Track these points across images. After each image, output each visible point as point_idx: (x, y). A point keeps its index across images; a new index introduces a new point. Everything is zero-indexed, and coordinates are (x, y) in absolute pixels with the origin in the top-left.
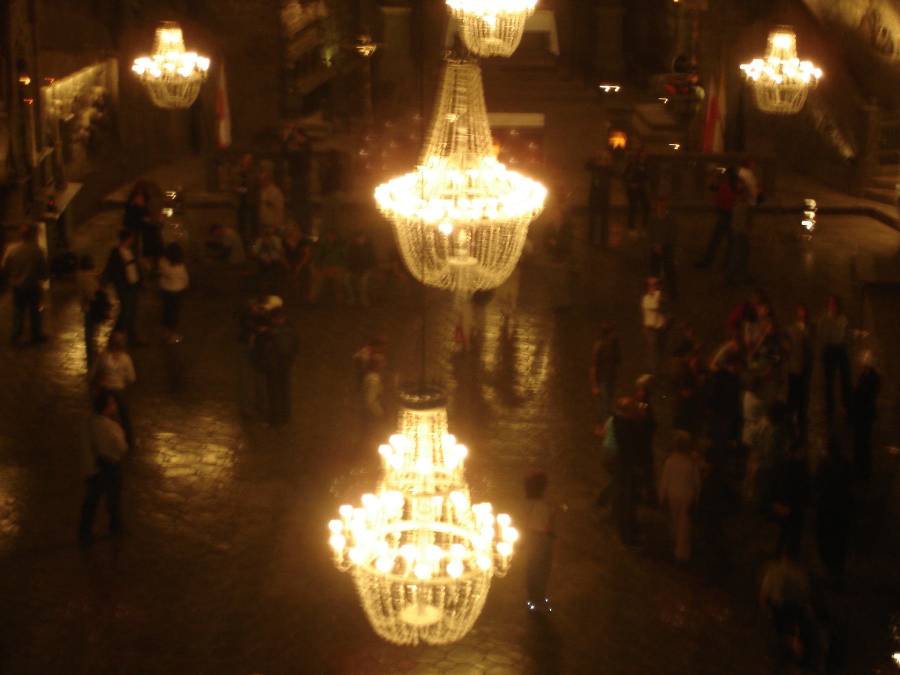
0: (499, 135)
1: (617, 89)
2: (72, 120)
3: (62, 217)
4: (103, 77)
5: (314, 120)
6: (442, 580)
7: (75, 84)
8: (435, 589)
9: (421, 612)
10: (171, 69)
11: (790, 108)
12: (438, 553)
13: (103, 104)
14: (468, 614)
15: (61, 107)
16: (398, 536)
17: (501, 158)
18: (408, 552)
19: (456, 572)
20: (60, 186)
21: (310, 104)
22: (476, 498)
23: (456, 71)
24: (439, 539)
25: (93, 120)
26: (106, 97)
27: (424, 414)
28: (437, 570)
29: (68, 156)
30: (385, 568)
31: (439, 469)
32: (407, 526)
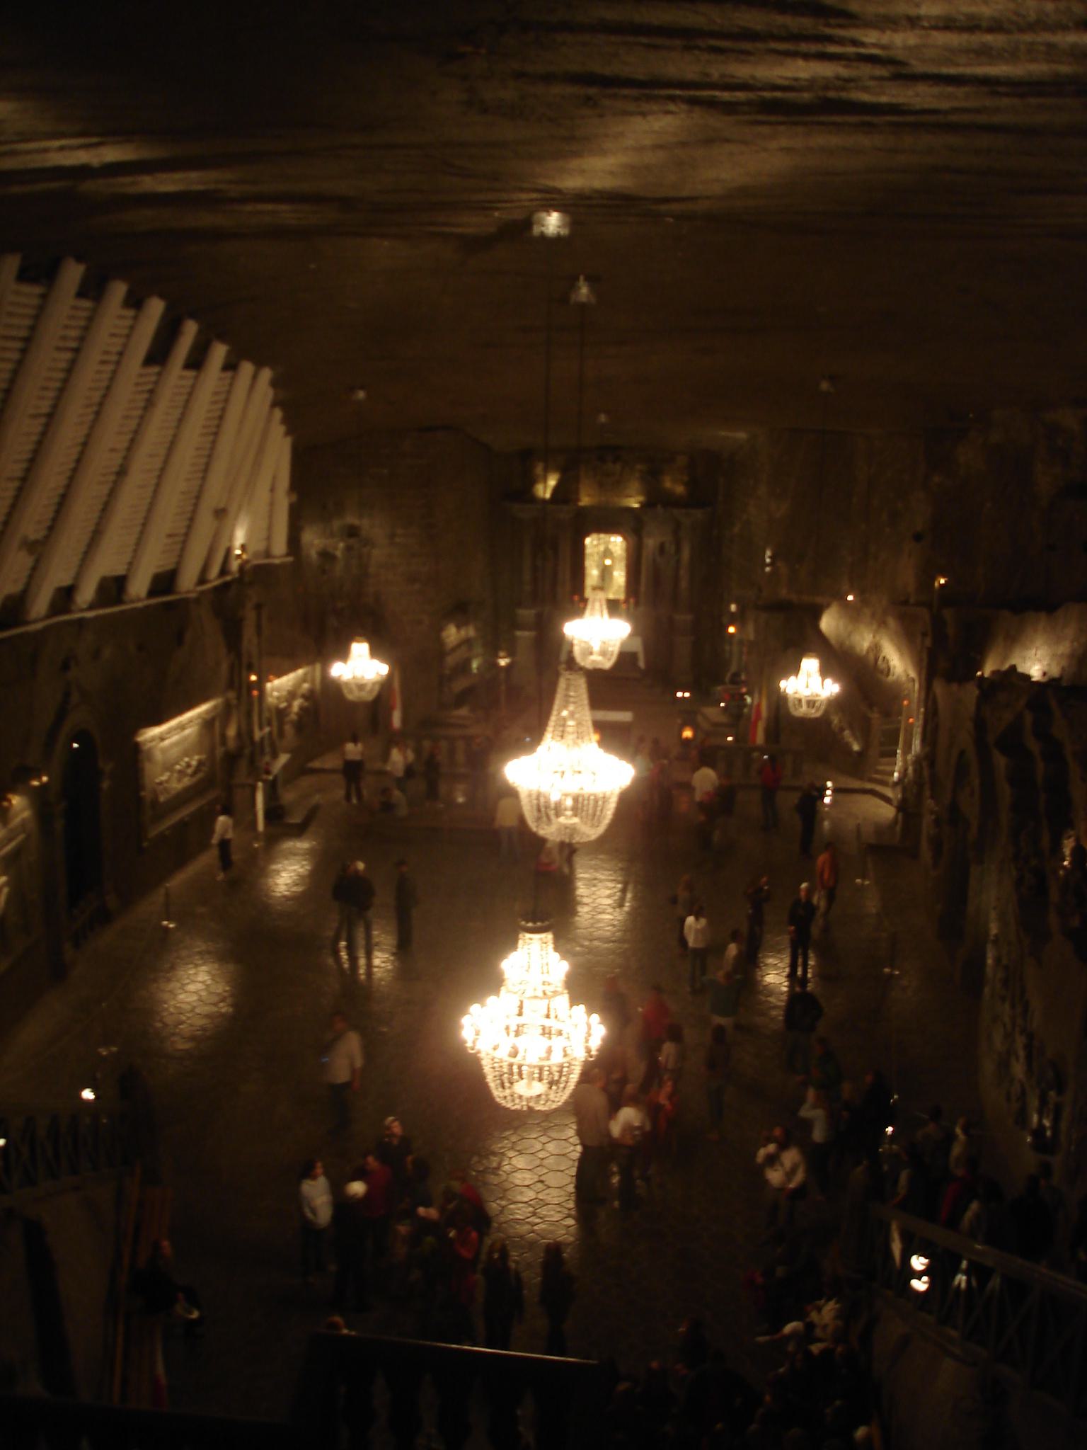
0: (599, 726)
1: (687, 695)
2: (286, 708)
3: (276, 778)
4: (309, 678)
5: (464, 711)
6: (545, 1063)
7: (288, 681)
8: (541, 1069)
9: (529, 1085)
10: (359, 674)
11: (814, 713)
12: (544, 1042)
13: (309, 696)
14: (564, 1088)
15: (278, 698)
16: (513, 1028)
17: (602, 743)
18: (521, 1042)
19: (557, 1058)
20: (275, 756)
21: (461, 700)
22: (574, 1001)
23: (568, 679)
24: (546, 1032)
25: (302, 708)
26: (312, 691)
27: (536, 936)
28: (544, 1055)
29: (281, 733)
30: (503, 1054)
31: (546, 978)
32: (521, 1020)
